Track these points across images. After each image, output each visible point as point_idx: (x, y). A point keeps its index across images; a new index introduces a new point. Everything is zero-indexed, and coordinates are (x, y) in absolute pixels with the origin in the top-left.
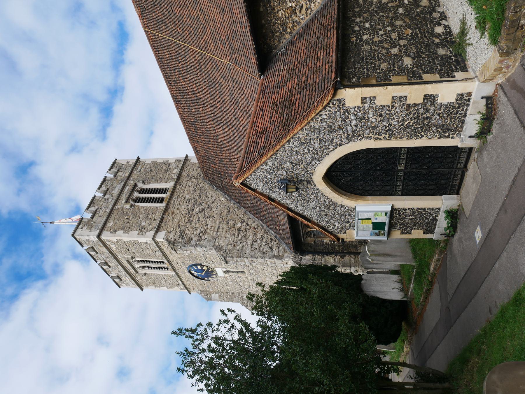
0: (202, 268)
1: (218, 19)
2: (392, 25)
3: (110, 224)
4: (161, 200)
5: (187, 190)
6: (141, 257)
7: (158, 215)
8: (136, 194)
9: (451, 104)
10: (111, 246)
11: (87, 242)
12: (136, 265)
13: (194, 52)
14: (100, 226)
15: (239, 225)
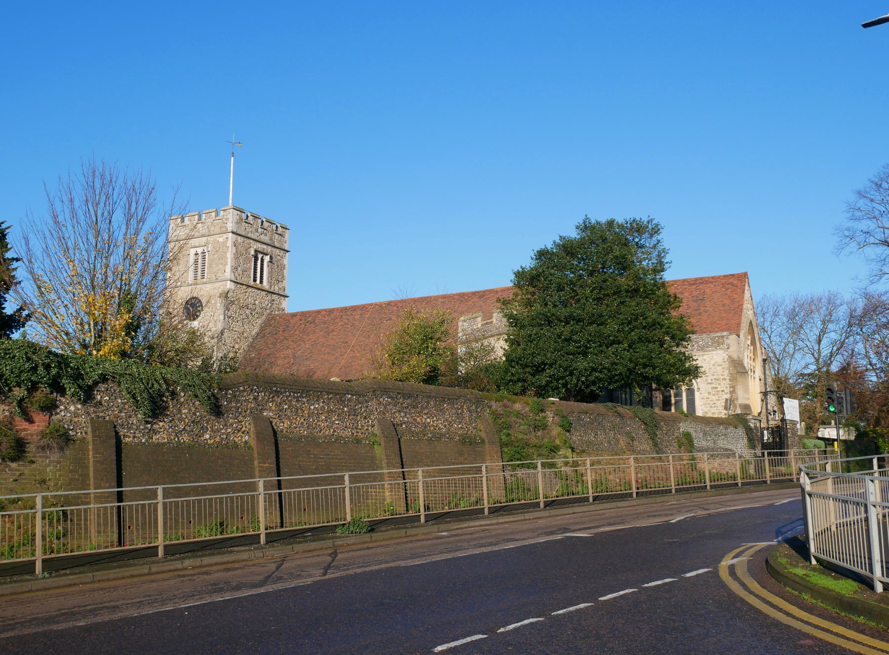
4: (255, 280)
5: (261, 300)
7: (244, 280)
8: (260, 256)
15: (237, 347)
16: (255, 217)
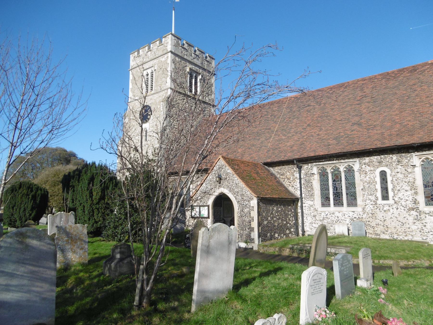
0: (149, 115)
1: (288, 144)
2: (279, 218)
3: (177, 59)
6: (155, 76)
9: (251, 237)
10: (164, 58)
11: (166, 42)
12: (149, 71)
13: (275, 128)
14: (176, 52)
16: (189, 45)
